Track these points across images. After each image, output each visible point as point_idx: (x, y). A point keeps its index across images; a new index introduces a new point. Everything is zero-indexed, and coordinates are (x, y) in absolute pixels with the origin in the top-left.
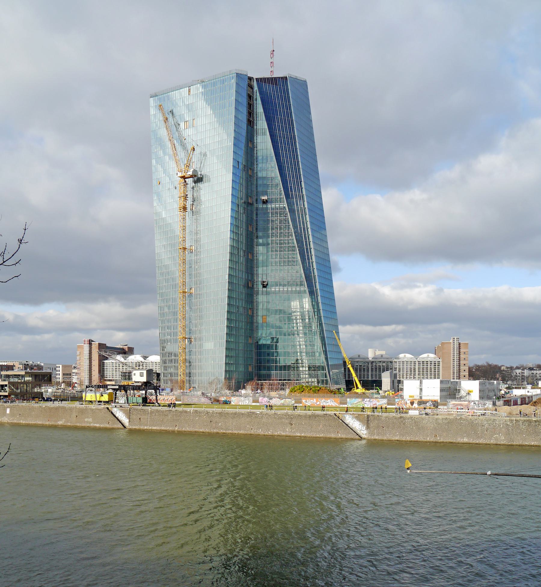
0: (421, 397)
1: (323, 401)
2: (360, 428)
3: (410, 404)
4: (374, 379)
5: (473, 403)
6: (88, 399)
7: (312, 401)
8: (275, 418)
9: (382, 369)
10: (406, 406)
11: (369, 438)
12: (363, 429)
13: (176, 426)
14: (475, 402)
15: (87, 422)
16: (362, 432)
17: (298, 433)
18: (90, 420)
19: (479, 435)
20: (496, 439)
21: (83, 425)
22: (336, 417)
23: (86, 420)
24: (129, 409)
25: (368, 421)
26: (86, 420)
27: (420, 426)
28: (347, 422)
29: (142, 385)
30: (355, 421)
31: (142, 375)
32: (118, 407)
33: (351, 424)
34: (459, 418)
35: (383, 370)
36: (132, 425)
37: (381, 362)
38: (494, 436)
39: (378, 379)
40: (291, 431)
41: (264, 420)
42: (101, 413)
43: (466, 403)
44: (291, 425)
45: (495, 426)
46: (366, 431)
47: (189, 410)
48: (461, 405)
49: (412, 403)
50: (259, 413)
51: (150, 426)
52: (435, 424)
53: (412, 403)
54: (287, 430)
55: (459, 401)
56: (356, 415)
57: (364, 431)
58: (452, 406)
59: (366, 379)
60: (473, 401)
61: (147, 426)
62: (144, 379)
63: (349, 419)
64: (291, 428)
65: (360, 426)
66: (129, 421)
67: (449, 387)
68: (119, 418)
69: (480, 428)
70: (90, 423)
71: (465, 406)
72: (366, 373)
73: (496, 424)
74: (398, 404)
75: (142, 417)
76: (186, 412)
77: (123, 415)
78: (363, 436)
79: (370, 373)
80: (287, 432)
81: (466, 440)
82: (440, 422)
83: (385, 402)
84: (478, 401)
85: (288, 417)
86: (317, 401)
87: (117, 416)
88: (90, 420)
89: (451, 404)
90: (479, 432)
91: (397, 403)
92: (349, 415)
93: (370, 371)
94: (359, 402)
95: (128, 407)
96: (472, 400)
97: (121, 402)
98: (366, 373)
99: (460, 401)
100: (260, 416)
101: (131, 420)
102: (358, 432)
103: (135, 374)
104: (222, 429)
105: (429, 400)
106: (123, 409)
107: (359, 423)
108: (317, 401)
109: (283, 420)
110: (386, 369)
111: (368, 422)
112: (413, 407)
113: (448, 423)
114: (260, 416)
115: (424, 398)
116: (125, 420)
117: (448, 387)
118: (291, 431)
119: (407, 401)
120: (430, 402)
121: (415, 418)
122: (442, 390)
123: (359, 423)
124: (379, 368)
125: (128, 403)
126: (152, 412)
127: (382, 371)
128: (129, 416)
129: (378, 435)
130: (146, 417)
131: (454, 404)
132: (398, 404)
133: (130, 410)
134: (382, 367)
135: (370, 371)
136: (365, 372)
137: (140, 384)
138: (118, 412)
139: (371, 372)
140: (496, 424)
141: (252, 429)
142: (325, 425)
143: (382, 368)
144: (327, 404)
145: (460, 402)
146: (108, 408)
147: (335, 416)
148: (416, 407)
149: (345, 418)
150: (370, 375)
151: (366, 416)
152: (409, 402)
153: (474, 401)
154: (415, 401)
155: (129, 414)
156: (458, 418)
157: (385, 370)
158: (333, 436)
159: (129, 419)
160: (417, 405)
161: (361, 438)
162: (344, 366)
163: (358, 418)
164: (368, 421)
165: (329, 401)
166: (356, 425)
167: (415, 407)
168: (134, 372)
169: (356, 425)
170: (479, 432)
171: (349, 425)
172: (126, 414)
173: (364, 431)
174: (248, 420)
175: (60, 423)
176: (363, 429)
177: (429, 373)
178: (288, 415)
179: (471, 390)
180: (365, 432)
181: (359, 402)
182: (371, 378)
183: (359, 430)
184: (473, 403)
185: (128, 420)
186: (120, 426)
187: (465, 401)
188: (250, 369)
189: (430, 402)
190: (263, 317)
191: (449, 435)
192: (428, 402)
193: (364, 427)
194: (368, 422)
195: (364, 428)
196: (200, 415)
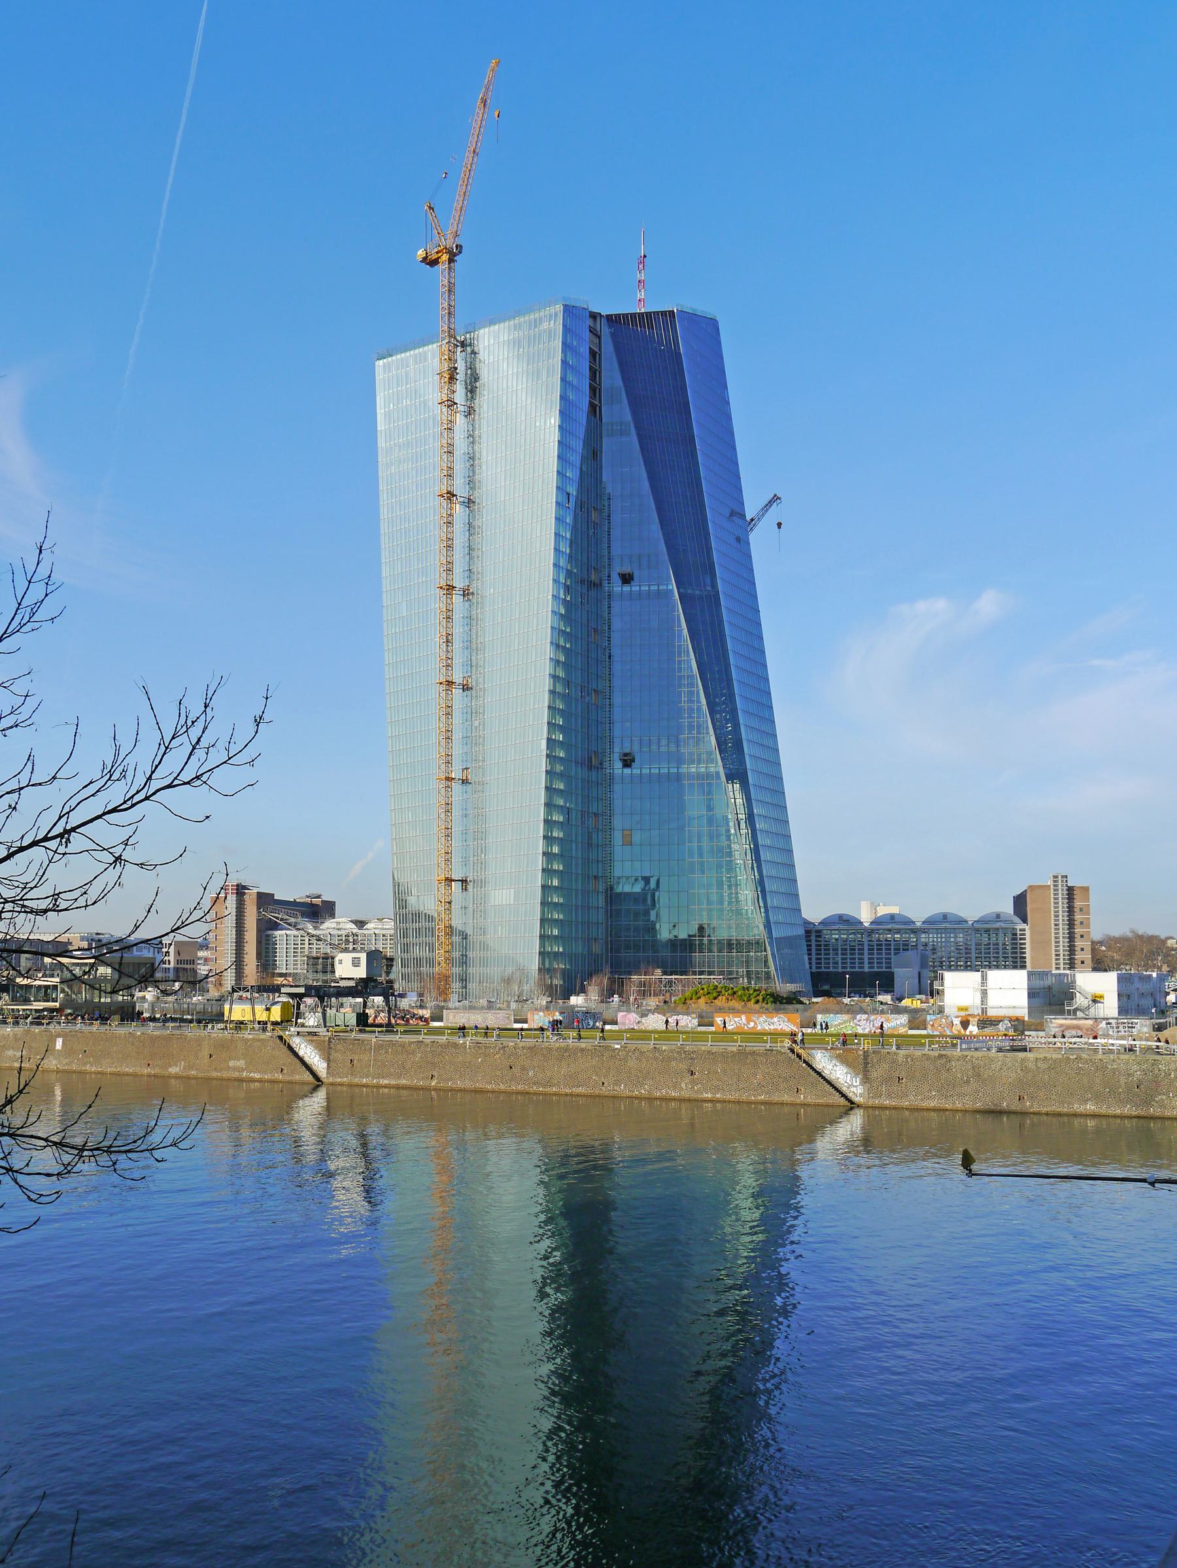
0: (984, 1011)
1: (761, 1019)
2: (848, 1081)
3: (960, 1027)
4: (876, 970)
5: (1104, 1022)
6: (236, 1016)
7: (736, 1019)
8: (655, 1059)
9: (892, 947)
10: (951, 1031)
11: (870, 1104)
12: (854, 1084)
13: (432, 1076)
14: (1110, 1021)
15: (235, 1069)
16: (854, 1089)
17: (707, 1093)
18: (241, 1063)
19: (1122, 1096)
21: (225, 1075)
22: (793, 1057)
23: (231, 1063)
25: (866, 1064)
26: (231, 1063)
28: (819, 1067)
29: (357, 986)
31: (356, 963)
32: (304, 1036)
34: (1075, 1057)
35: (895, 949)
37: (889, 930)
39: (884, 970)
40: (693, 1087)
41: (632, 1063)
43: (1090, 1022)
47: (461, 1042)
48: (1078, 1027)
49: (965, 1024)
50: (618, 1047)
51: (373, 1078)
52: (1018, 1071)
53: (965, 1024)
54: (683, 1085)
55: (1072, 1019)
56: (838, 1052)
57: (856, 1086)
58: (1057, 1029)
59: (857, 970)
60: (1104, 1019)
61: (367, 1077)
62: (361, 972)
63: (822, 1060)
64: (693, 1083)
65: (849, 1075)
66: (329, 1067)
67: (1050, 988)
68: (306, 1059)
70: (241, 1070)
71: (1087, 1030)
72: (857, 956)
73: (1159, 1070)
74: (933, 1025)
75: (356, 1057)
76: (455, 1045)
77: (313, 1054)
78: (857, 1099)
79: (866, 957)
82: (1031, 1065)
83: (903, 1021)
84: (1117, 1019)
85: (683, 1055)
86: (749, 1021)
87: (301, 1053)
89: (1055, 1025)
90: (1120, 1090)
91: (931, 1023)
92: (824, 1051)
93: (866, 952)
94: (845, 1022)
95: (324, 1034)
96: (1102, 1016)
97: (311, 1023)
98: (857, 956)
99: (1075, 1019)
100: (620, 1053)
101: (332, 1064)
102: (844, 1089)
103: (341, 962)
104: (534, 1083)
105: (1005, 1017)
107: (845, 1071)
108: (749, 1021)
110: (901, 947)
112: (968, 1033)
114: (620, 1053)
115: (992, 1013)
116: (319, 1065)
117: (1046, 986)
119: (954, 1019)
120: (1006, 1022)
122: (1031, 994)
123: (845, 1071)
124: (886, 945)
125: (325, 1026)
126: (379, 1047)
127: (892, 951)
129: (889, 1096)
130: (365, 1057)
131: (1061, 1026)
132: (933, 1025)
133: (330, 1042)
134: (892, 943)
135: (866, 952)
136: (855, 954)
137: (352, 983)
138: (303, 1046)
139: (869, 954)
140: (1159, 1070)
141: (603, 1083)
143: (892, 945)
144: (772, 1027)
145: (1075, 1022)
146: (281, 1038)
147: (791, 1055)
148: (974, 1033)
150: (866, 961)
151: (861, 1053)
152: (957, 1022)
153: (1107, 1019)
154: (971, 1019)
155: (326, 1051)
156: (1071, 1057)
157: (899, 949)
158: (786, 1098)
159: (328, 1061)
160: (976, 1028)
161: (852, 1105)
162: (807, 941)
164: (866, 1064)
165: (776, 1019)
166: (839, 1073)
167: (971, 1032)
168: (340, 956)
169: (839, 1073)
170: (1120, 1090)
172: (320, 1050)
173: (856, 1086)
175: (173, 1070)
176: (854, 1084)
178: (685, 1052)
179: (1099, 993)
180: (860, 1090)
181: (845, 1022)
182: (870, 968)
183: (846, 1084)
184: (1104, 1022)
185: (325, 1065)
186: (308, 1077)
187: (1086, 1019)
188: (597, 948)
189: (1006, 1022)
190: (625, 833)
191: (1053, 1097)
192: (1001, 1021)
193: (858, 1079)
195: (857, 1081)
196: (487, 1051)
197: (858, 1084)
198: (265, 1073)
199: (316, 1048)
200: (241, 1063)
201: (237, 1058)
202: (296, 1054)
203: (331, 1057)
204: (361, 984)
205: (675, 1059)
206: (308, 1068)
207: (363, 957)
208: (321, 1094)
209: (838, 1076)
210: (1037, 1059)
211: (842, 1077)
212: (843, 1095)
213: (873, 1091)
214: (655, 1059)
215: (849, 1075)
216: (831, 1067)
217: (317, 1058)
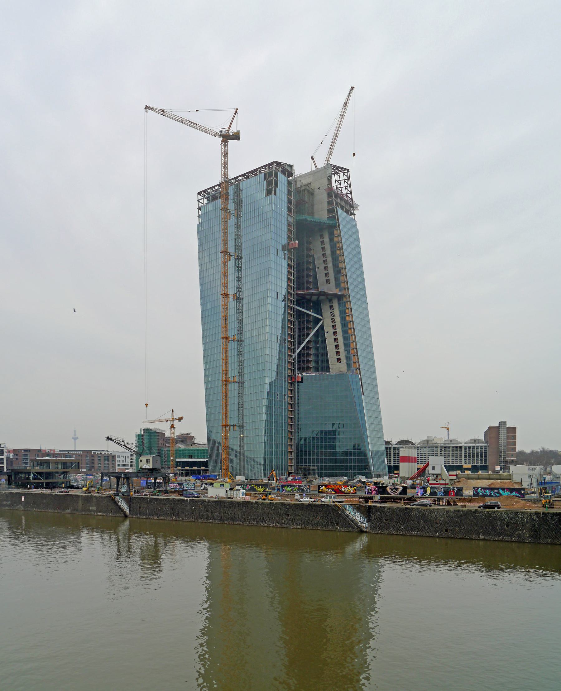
8: (270, 508)
15: (92, 511)
20: (519, 536)
24: (129, 497)
26: (91, 508)
27: (428, 519)
29: (147, 473)
30: (356, 512)
31: (148, 462)
33: (351, 516)
34: (474, 510)
36: (132, 514)
38: (516, 533)
40: (287, 523)
41: (260, 510)
42: (104, 501)
44: (288, 515)
45: (517, 521)
46: (367, 524)
51: (148, 516)
54: (283, 521)
61: (146, 515)
62: (150, 466)
63: (349, 511)
64: (288, 519)
68: (122, 506)
69: (499, 524)
70: (95, 511)
78: (365, 530)
80: (282, 523)
81: (482, 537)
82: (451, 514)
85: (284, 507)
87: (120, 503)
88: (94, 508)
101: (132, 509)
102: (359, 525)
103: (141, 461)
104: (217, 519)
106: (125, 497)
109: (279, 511)
111: (369, 514)
113: (461, 516)
116: (127, 510)
118: (287, 523)
121: (422, 509)
128: (129, 506)
129: (380, 529)
130: (145, 505)
133: (130, 498)
142: (323, 516)
149: (345, 509)
156: (472, 510)
163: (359, 509)
164: (369, 512)
166: (357, 517)
168: (141, 458)
169: (357, 517)
170: (497, 528)
171: (349, 517)
172: (127, 502)
174: (243, 510)
177: (475, 458)
178: (284, 505)
180: (366, 525)
183: (360, 522)
185: (128, 510)
191: (462, 530)
194: (369, 514)
197: (366, 522)
198: (104, 512)
199: (126, 501)
200: (94, 508)
201: (92, 506)
202: (117, 504)
203: (131, 506)
204: (150, 471)
205: (280, 508)
206: (122, 510)
207: (151, 459)
208: (127, 523)
209: (356, 518)
210: (454, 511)
211: (358, 519)
212: (358, 527)
213: (373, 527)
214: (270, 508)
215: (362, 518)
216: (353, 513)
217: (126, 506)
